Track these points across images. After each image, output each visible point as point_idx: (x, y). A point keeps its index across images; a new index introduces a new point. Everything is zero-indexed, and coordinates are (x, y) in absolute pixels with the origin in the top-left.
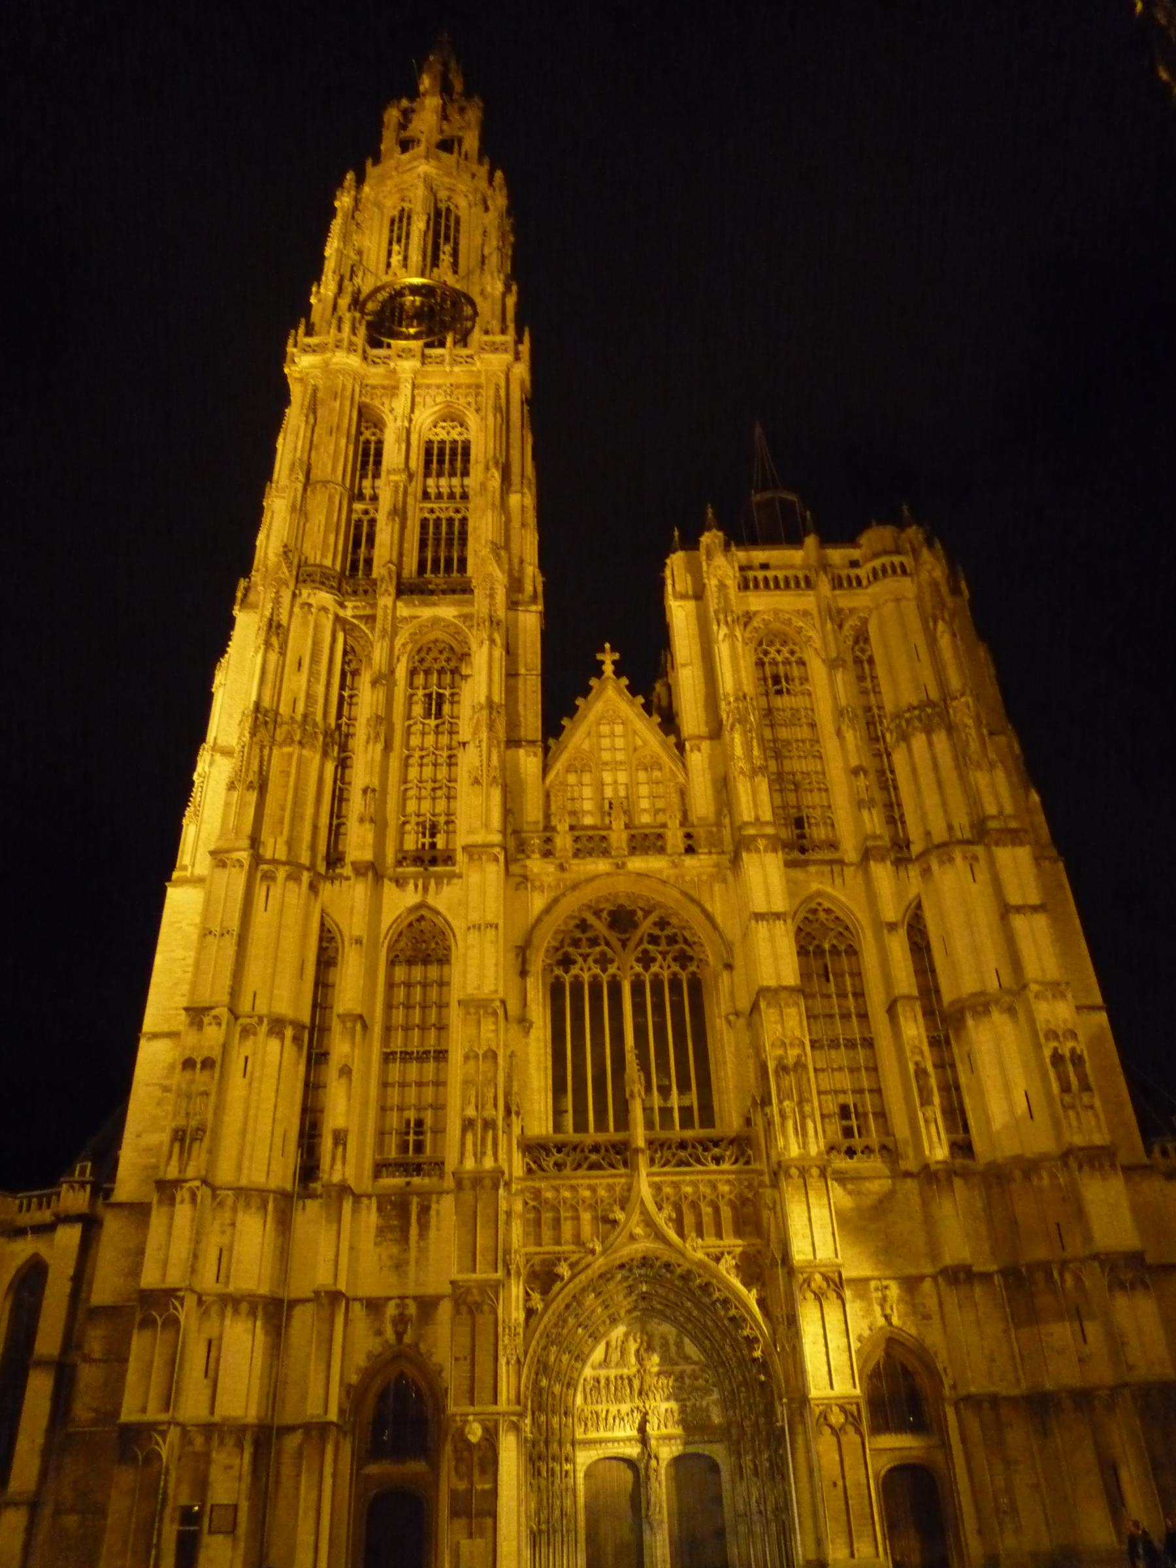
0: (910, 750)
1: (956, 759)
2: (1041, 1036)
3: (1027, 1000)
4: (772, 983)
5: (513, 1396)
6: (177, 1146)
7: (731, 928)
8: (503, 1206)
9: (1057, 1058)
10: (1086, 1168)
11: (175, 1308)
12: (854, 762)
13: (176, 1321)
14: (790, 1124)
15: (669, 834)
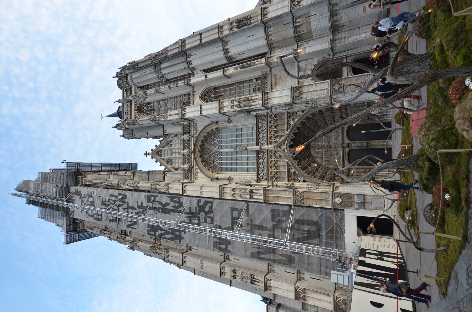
0: (166, 74)
1: (167, 61)
2: (232, 32)
3: (223, 37)
4: (218, 109)
5: (328, 187)
6: (255, 283)
7: (208, 122)
8: (275, 188)
9: (238, 27)
10: (267, 16)
11: (300, 289)
12: (168, 88)
13: (304, 289)
14: (253, 104)
15: (185, 139)
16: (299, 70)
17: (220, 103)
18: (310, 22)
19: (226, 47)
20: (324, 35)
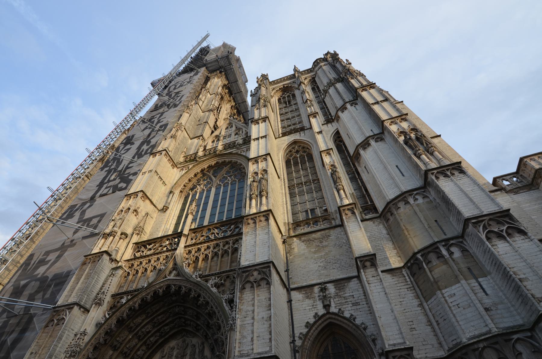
0: (329, 93)
10: (441, 177)
16: (337, 282)
17: (264, 157)
18: (459, 282)
19: (372, 142)
20: (438, 331)
